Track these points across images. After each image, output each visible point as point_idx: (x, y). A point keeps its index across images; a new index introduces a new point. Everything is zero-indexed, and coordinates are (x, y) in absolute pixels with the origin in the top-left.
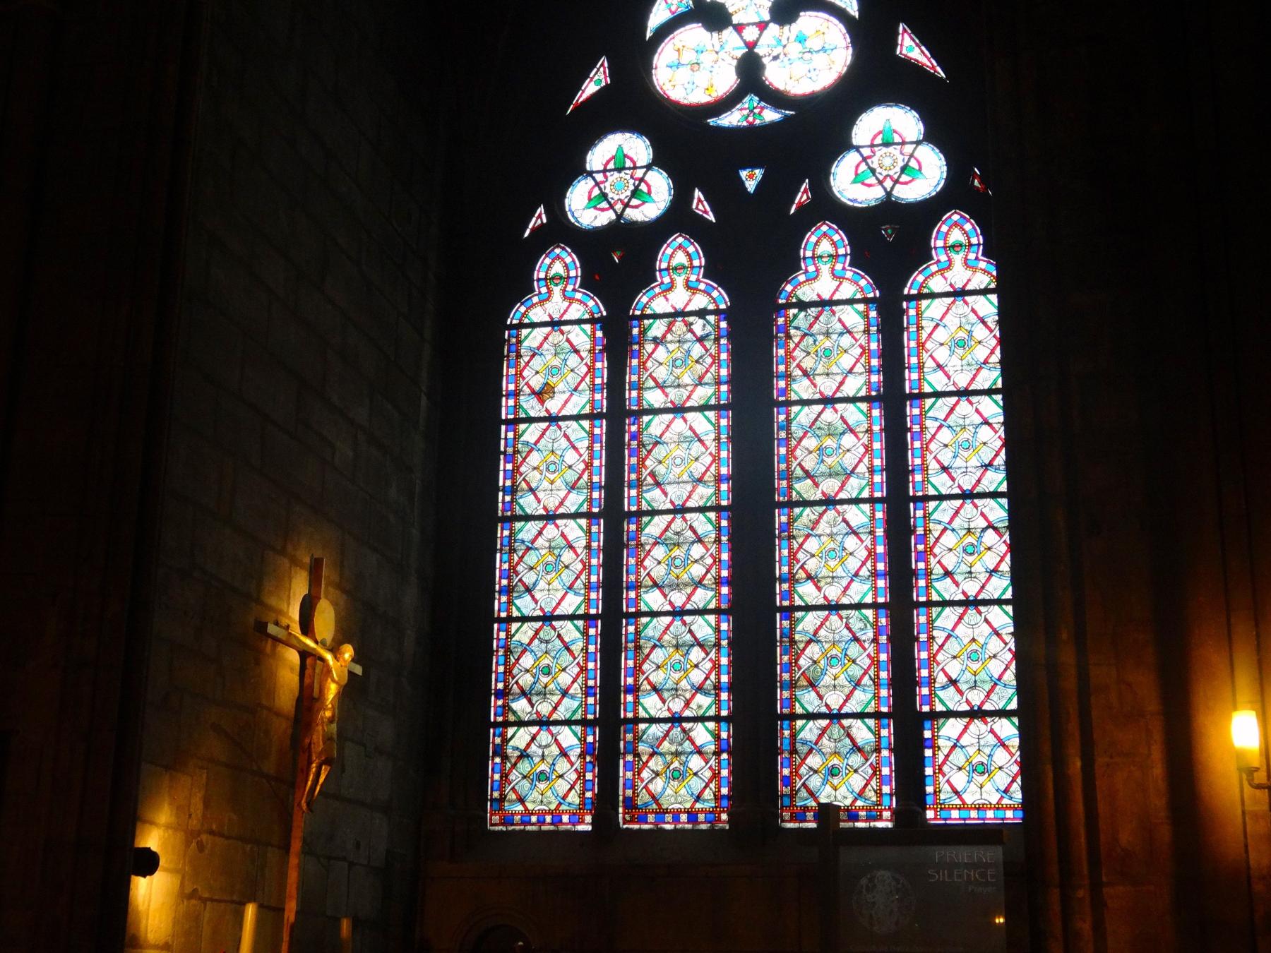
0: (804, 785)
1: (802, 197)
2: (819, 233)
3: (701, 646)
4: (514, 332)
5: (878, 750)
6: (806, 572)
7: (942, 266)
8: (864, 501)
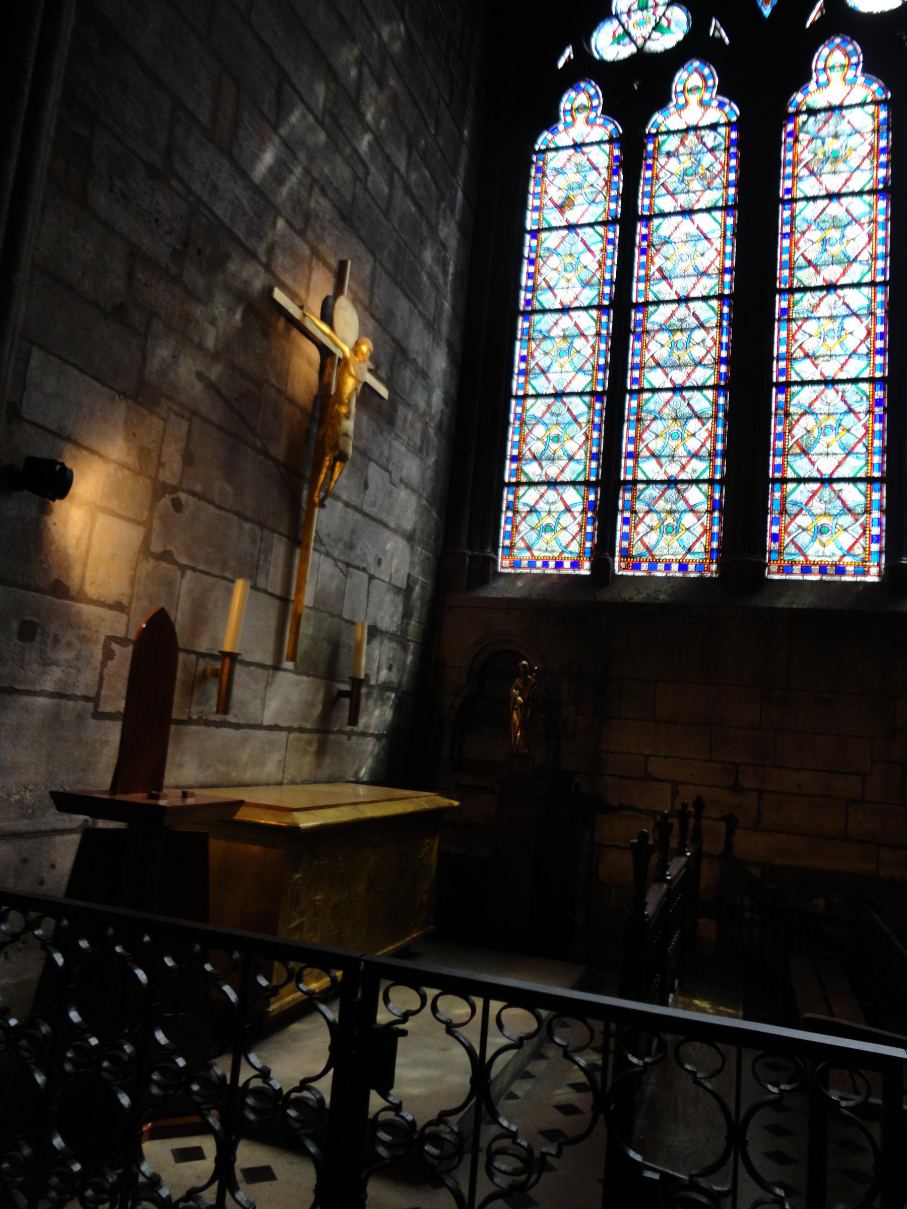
3: (700, 418)
4: (541, 156)
5: (868, 511)
6: (803, 350)
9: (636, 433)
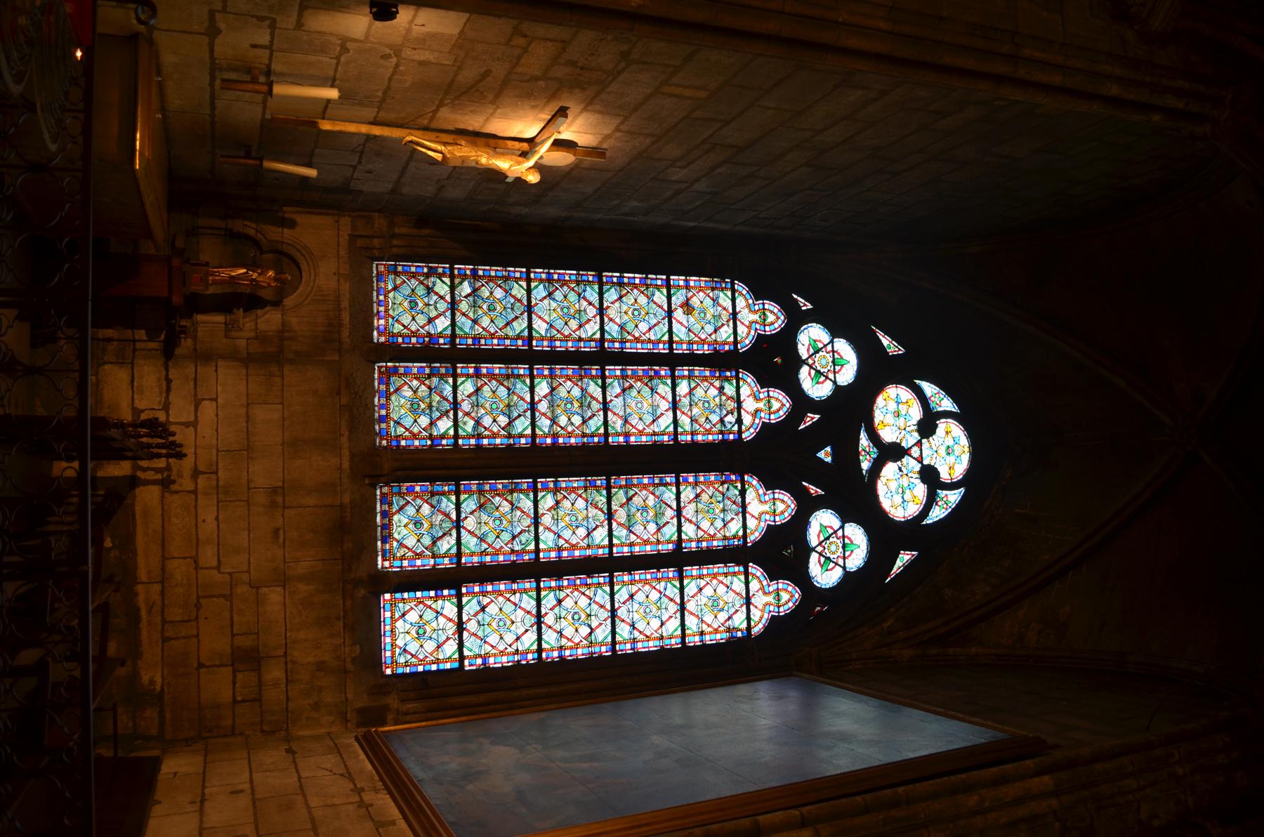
1: (813, 490)
2: (789, 502)
3: (509, 424)
5: (434, 556)
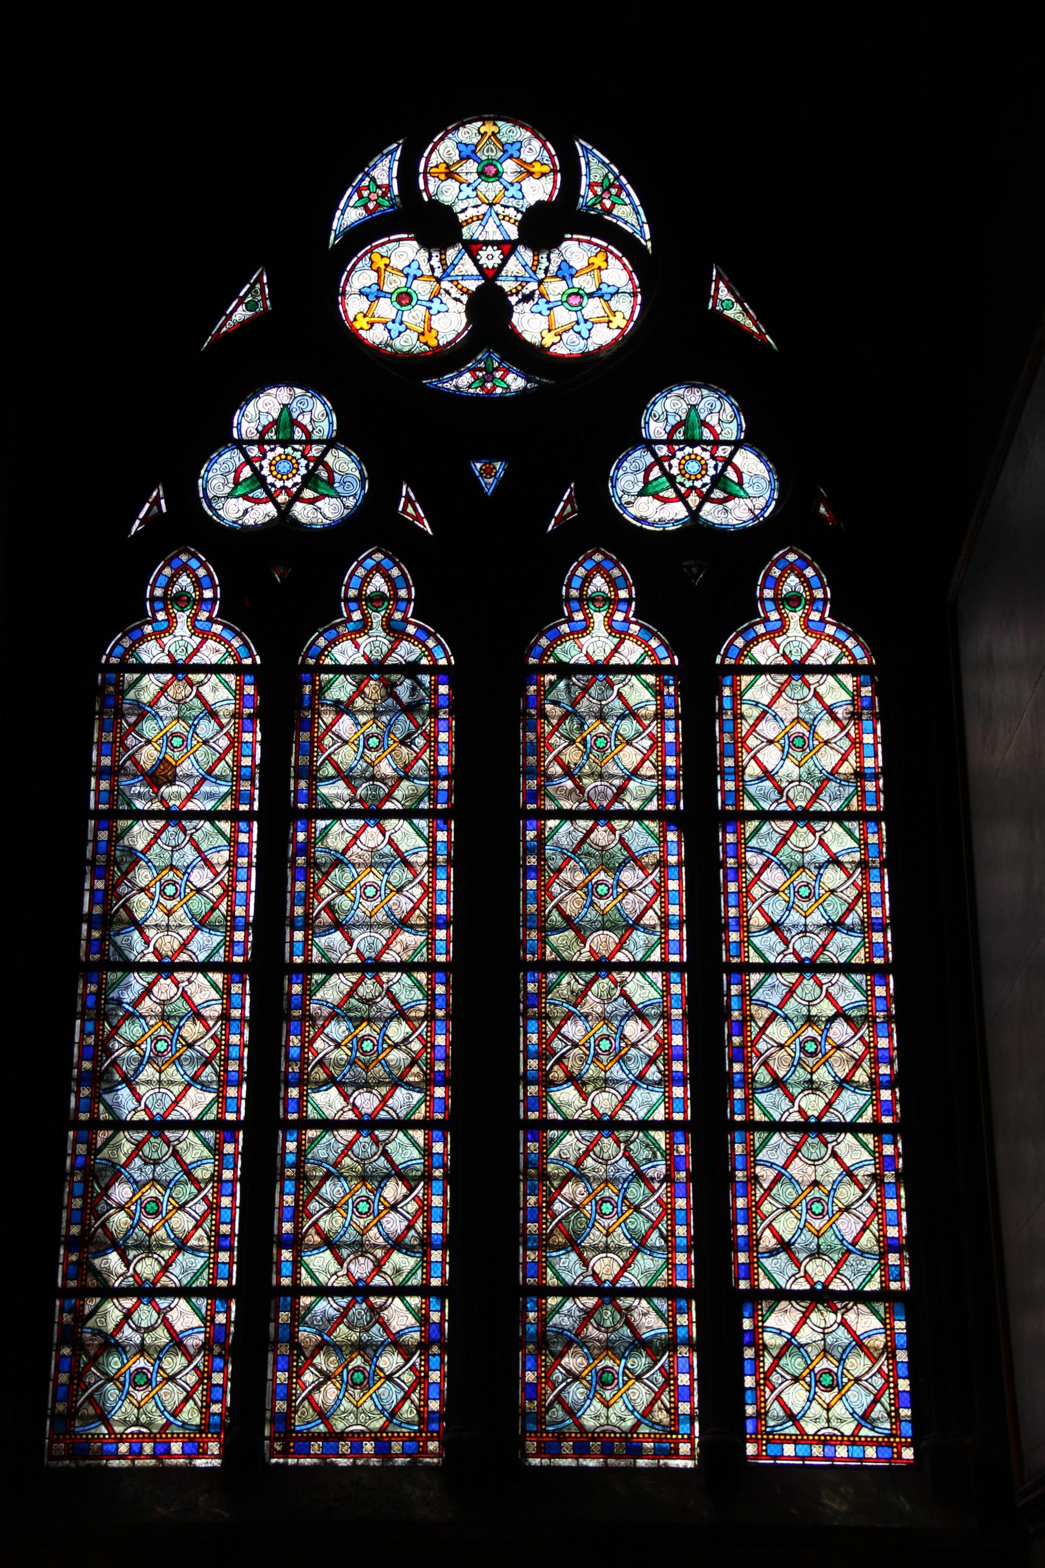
0: (558, 1398)
2: (589, 565)
6: (565, 1069)
7: (771, 626)
8: (654, 967)
9: (297, 1200)
